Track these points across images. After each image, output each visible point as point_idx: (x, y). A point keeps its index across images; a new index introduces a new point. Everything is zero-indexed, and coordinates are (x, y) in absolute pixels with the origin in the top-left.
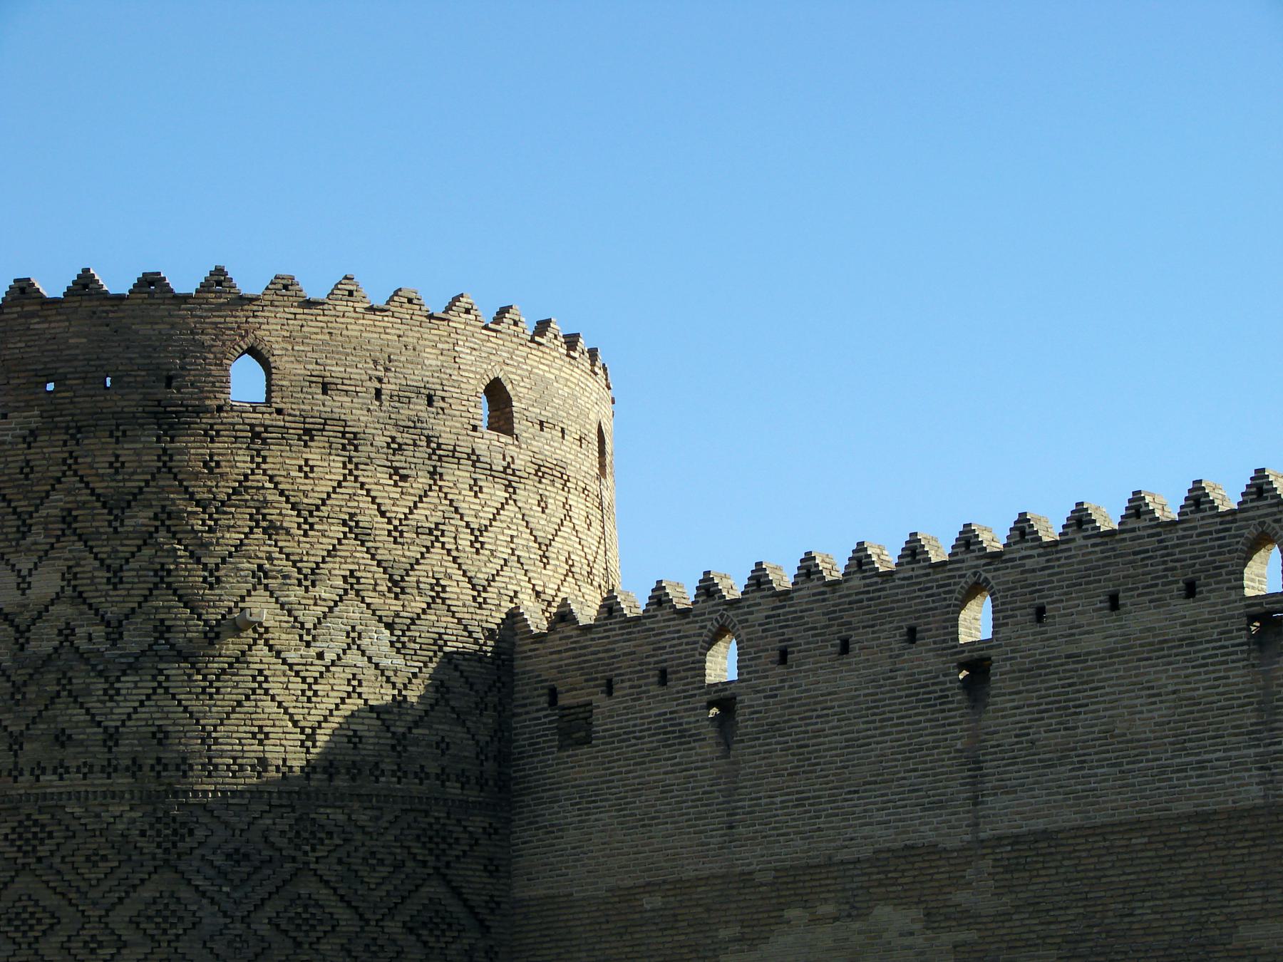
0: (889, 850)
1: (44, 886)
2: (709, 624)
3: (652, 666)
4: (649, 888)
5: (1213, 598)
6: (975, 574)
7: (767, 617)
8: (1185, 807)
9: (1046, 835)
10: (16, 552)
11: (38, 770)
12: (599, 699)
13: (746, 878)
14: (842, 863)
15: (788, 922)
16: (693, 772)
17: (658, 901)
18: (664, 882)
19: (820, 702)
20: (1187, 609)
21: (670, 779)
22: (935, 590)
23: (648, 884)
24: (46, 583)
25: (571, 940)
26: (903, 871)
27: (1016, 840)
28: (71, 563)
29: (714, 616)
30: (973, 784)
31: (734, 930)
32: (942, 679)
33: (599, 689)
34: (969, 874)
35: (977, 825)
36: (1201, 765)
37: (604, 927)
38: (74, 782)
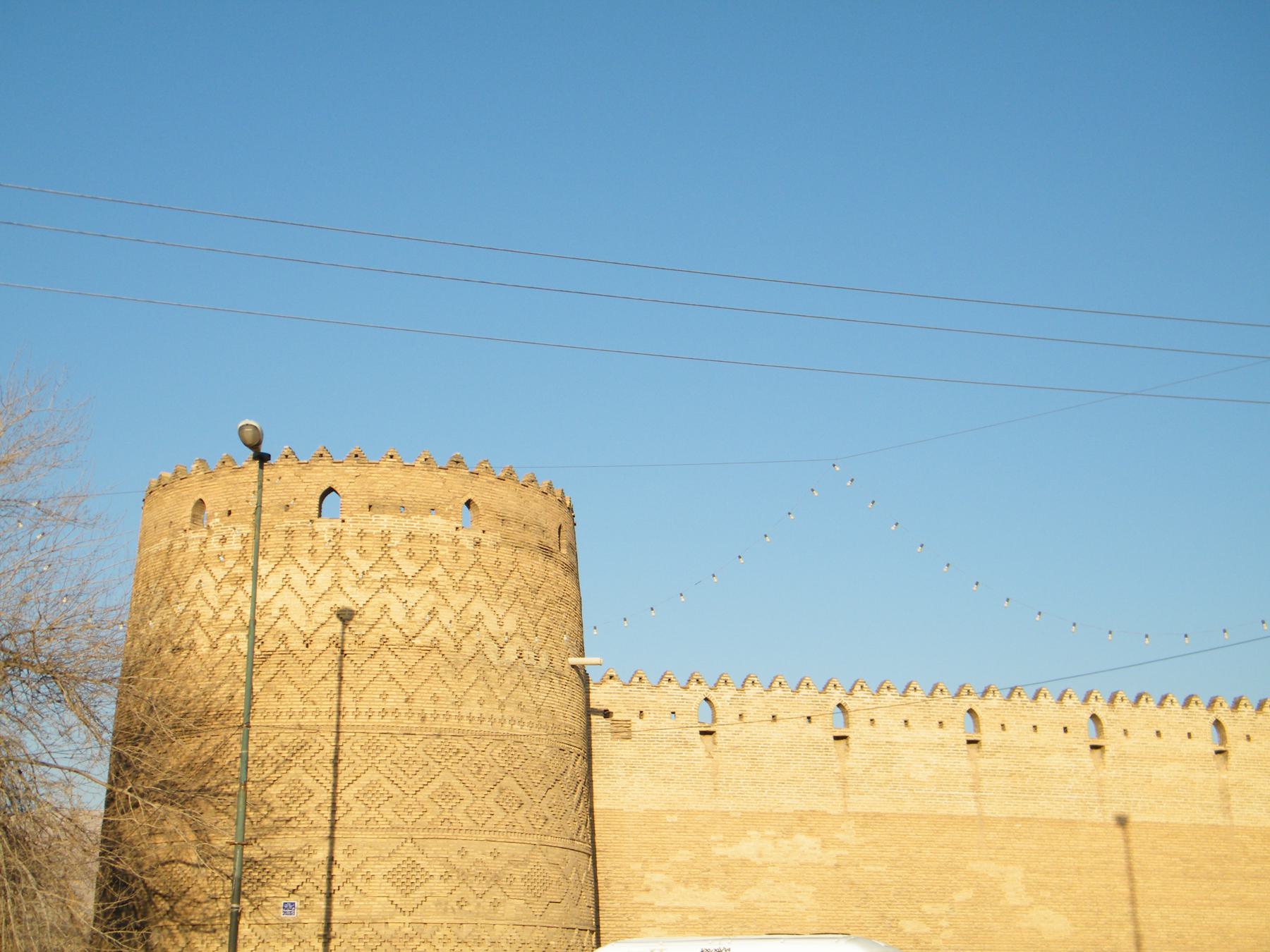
0: (802, 811)
1: (515, 783)
2: (699, 696)
3: (667, 709)
4: (671, 812)
5: (951, 730)
6: (840, 700)
7: (732, 698)
8: (944, 812)
9: (878, 815)
10: (495, 605)
11: (512, 721)
12: (635, 719)
13: (726, 814)
14: (777, 813)
15: (749, 836)
16: (692, 762)
17: (675, 818)
18: (678, 810)
19: (763, 741)
20: (939, 732)
21: (678, 763)
22: (820, 703)
23: (669, 810)
24: (510, 625)
25: (623, 831)
26: (810, 821)
27: (865, 815)
28: (520, 617)
29: (702, 693)
30: (844, 788)
31: (721, 837)
32: (825, 741)
33: (636, 715)
34: (843, 826)
35: (846, 806)
36: (950, 796)
37: (643, 827)
38: (526, 730)
